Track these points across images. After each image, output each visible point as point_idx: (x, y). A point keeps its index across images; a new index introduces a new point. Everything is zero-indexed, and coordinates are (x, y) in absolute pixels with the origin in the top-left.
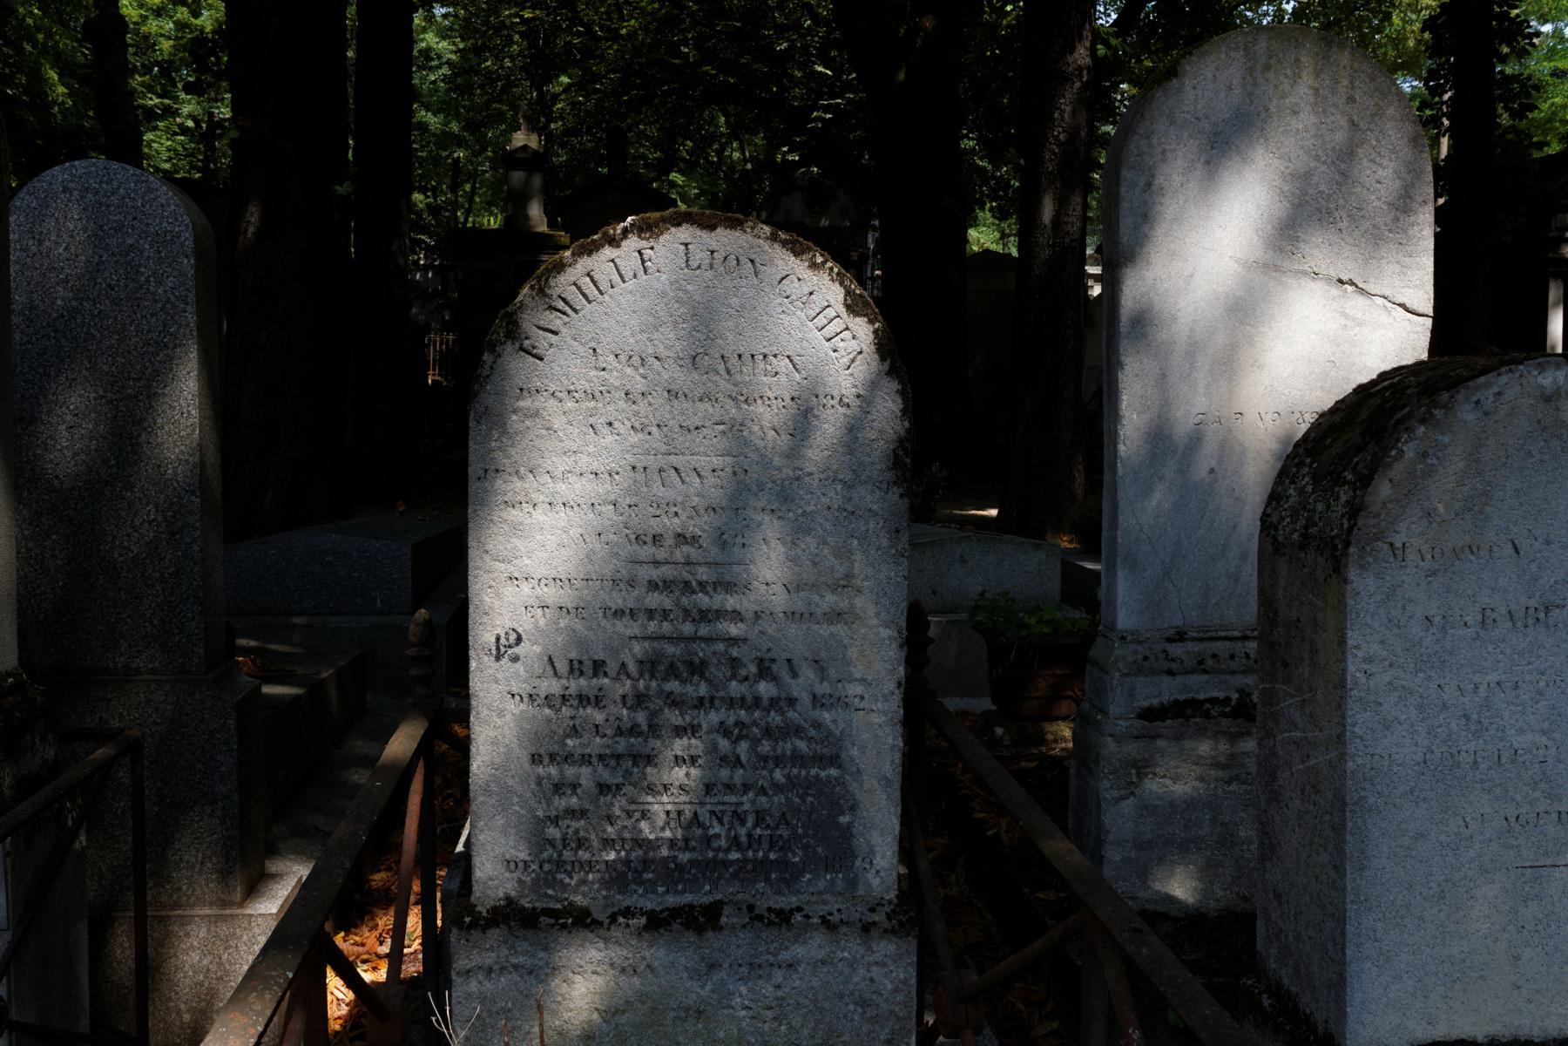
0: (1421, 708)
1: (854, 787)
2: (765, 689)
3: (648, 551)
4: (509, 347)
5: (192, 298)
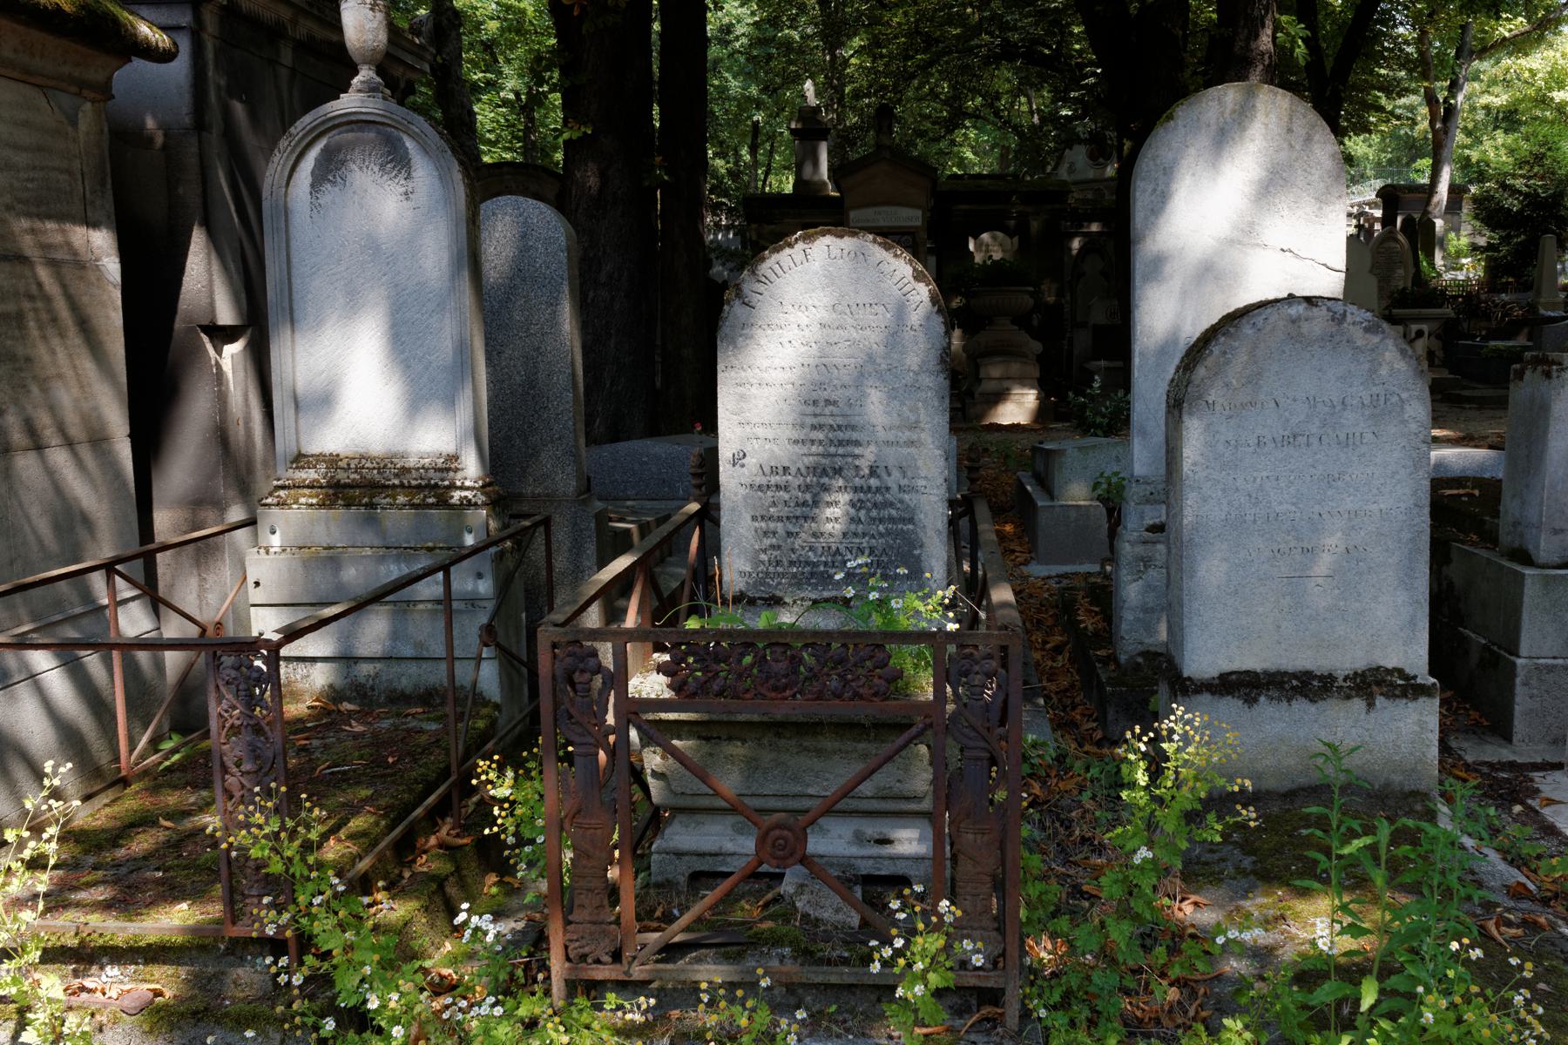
0: (1224, 490)
1: (921, 535)
2: (873, 482)
3: (810, 409)
4: (737, 302)
5: (566, 276)
